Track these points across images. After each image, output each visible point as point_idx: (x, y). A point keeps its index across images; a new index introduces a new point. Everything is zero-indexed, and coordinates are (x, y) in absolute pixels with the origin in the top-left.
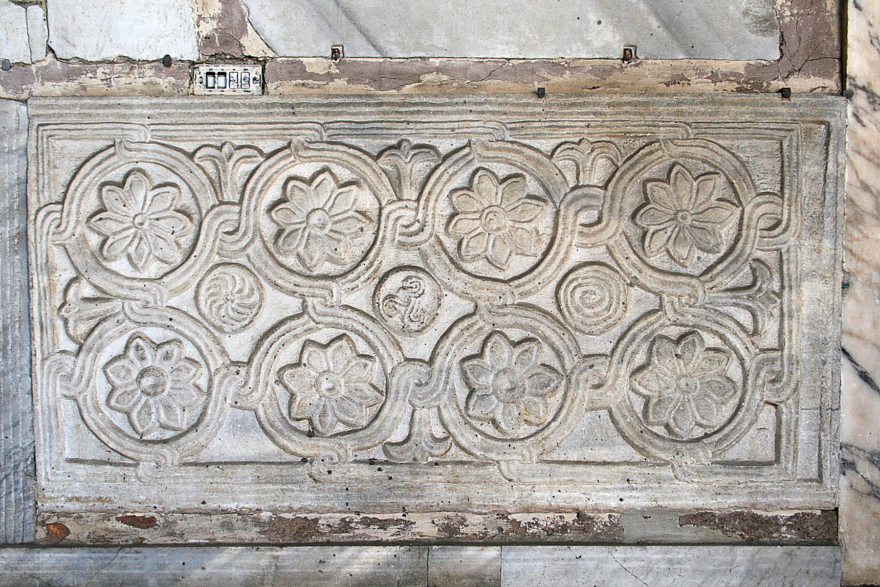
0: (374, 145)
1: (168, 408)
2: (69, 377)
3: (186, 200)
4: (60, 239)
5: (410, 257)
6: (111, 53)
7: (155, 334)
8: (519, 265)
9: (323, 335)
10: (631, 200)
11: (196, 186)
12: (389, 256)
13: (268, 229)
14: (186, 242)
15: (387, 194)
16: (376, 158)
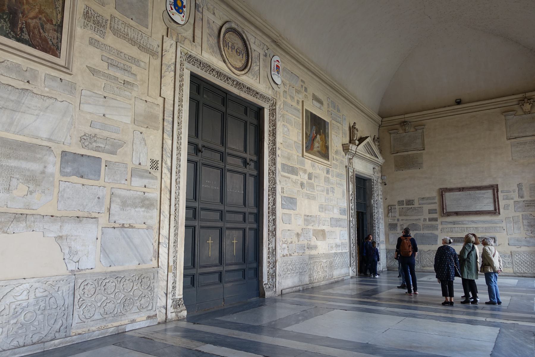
0: (115, 277)
1: (90, 314)
2: (78, 312)
3: (94, 286)
4: (79, 293)
5: (119, 291)
6: (86, 268)
7: (89, 304)
8: (130, 290)
9: (108, 302)
10: (141, 281)
11: (96, 284)
12: (116, 290)
13: (104, 289)
14: (94, 292)
15: (117, 283)
16: (116, 279)
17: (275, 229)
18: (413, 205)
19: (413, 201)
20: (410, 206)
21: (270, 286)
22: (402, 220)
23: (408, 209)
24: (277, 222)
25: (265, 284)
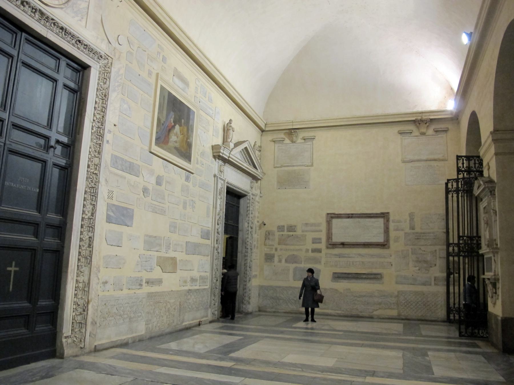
17: (91, 252)
18: (295, 231)
19: (295, 226)
20: (291, 233)
21: (75, 339)
22: (281, 250)
23: (289, 236)
24: (94, 242)
25: (66, 337)
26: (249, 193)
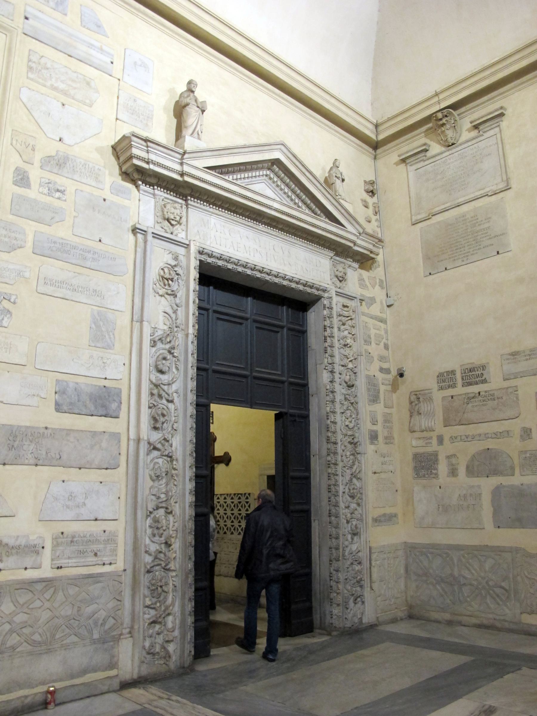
18: (484, 381)
19: (484, 367)
20: (474, 389)
22: (453, 439)
23: (470, 398)
26: (324, 291)
